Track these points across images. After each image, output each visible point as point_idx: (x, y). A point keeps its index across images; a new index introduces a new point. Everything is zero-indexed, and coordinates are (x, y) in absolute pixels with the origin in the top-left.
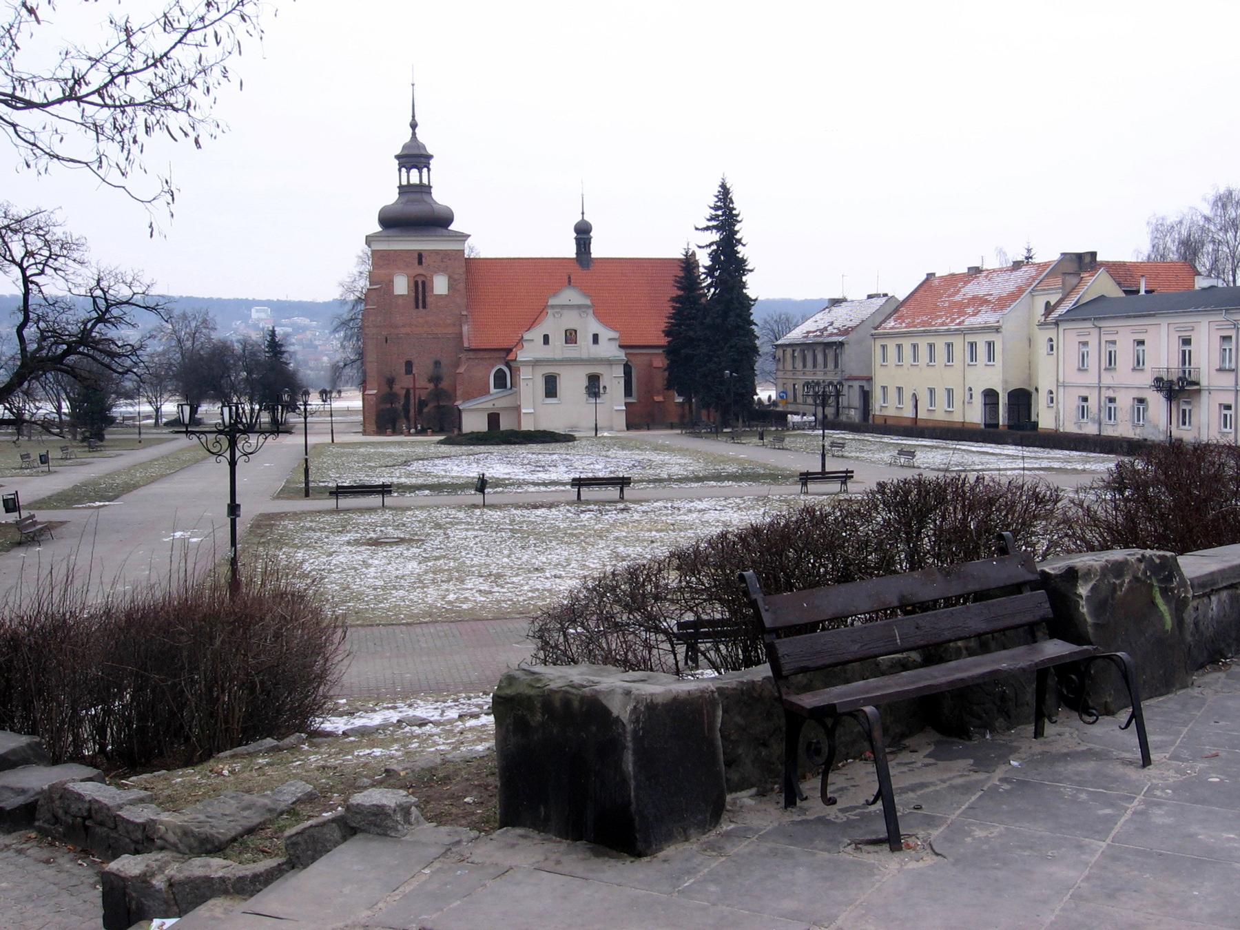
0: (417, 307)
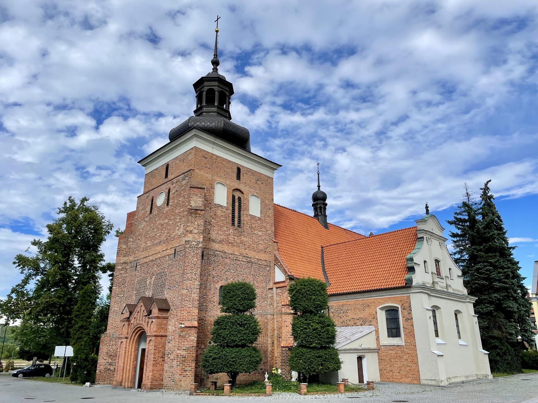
0: (233, 224)
